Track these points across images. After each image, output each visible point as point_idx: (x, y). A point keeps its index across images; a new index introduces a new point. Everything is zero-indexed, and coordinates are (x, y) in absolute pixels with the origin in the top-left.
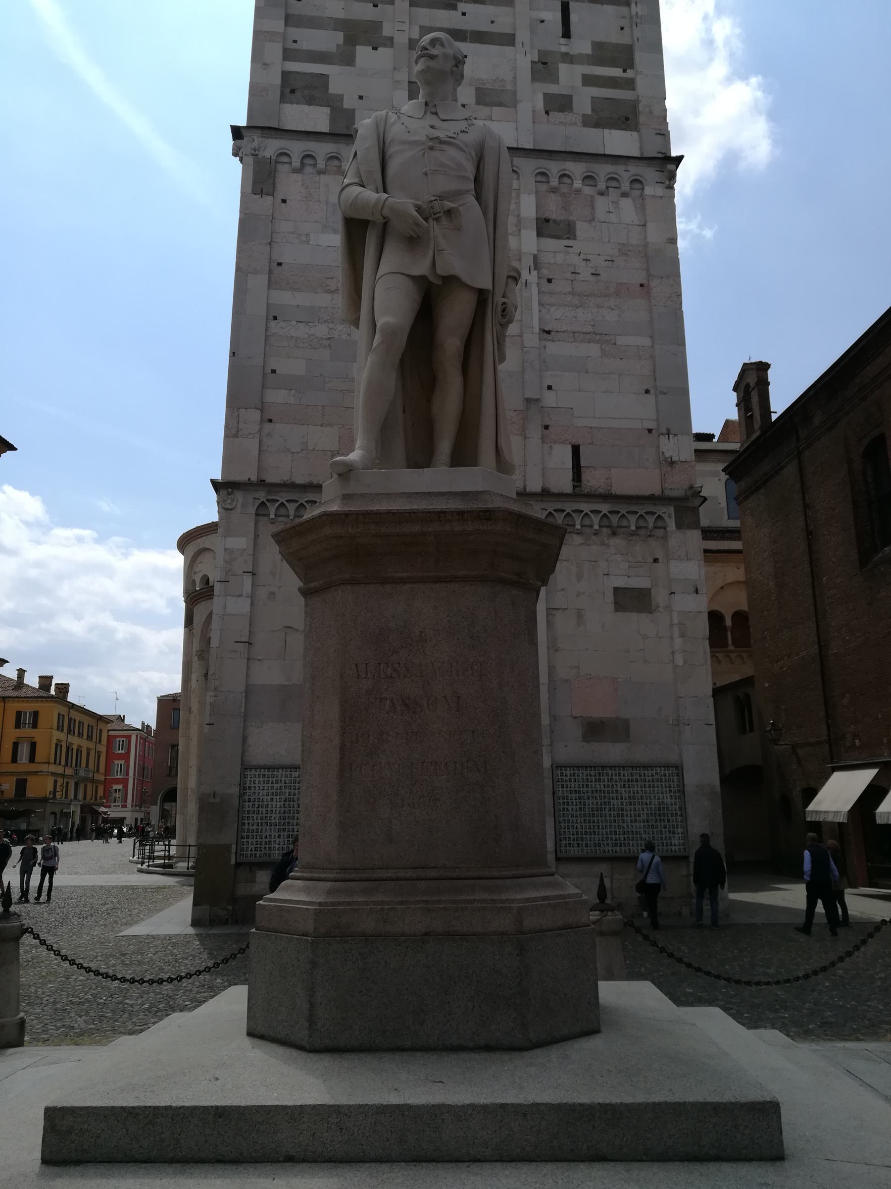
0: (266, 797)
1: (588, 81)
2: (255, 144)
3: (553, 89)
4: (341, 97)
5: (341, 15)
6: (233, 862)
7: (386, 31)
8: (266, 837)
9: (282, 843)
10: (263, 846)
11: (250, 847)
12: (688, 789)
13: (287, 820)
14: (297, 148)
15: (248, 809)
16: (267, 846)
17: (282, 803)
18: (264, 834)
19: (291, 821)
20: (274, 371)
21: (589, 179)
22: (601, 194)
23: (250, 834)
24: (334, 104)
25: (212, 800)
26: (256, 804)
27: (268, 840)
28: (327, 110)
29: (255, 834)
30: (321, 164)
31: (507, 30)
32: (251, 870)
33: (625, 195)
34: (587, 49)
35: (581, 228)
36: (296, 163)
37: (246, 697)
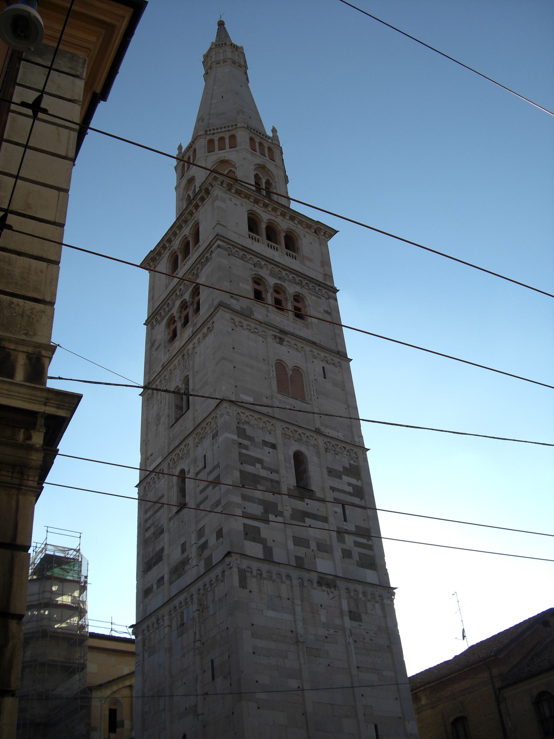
1: (357, 544)
2: (239, 562)
3: (345, 547)
4: (266, 539)
5: (261, 497)
7: (280, 509)
14: (255, 565)
20: (257, 681)
21: (364, 593)
22: (369, 601)
24: (263, 541)
28: (261, 546)
30: (265, 575)
31: (325, 515)
33: (377, 602)
34: (353, 529)
35: (363, 616)
36: (255, 573)
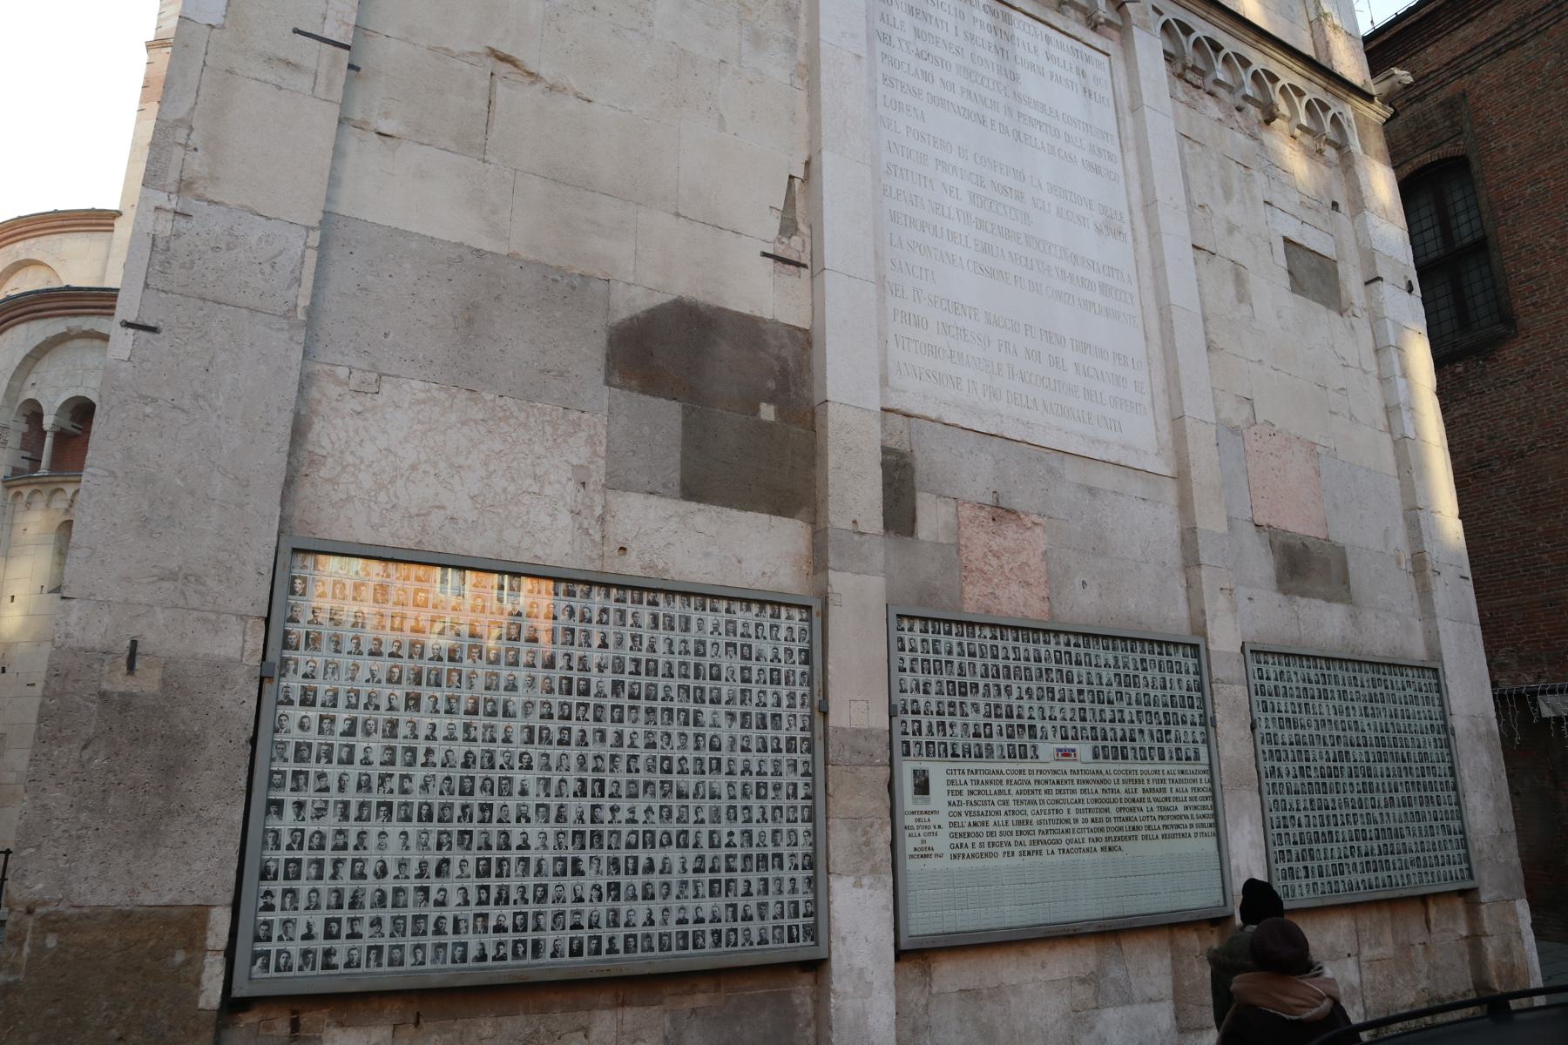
0: (385, 691)
6: (211, 994)
8: (382, 872)
9: (455, 898)
10: (368, 914)
11: (302, 918)
12: (1459, 723)
13: (479, 797)
15: (294, 736)
16: (387, 914)
17: (459, 721)
18: (372, 858)
19: (497, 801)
23: (305, 855)
25: (119, 683)
26: (342, 715)
27: (388, 885)
29: (328, 855)
32: (295, 1025)
37: (322, 248)
